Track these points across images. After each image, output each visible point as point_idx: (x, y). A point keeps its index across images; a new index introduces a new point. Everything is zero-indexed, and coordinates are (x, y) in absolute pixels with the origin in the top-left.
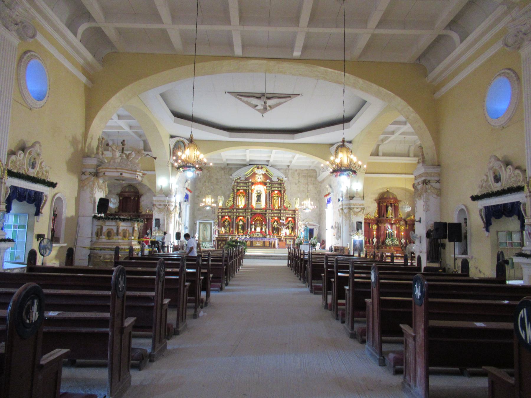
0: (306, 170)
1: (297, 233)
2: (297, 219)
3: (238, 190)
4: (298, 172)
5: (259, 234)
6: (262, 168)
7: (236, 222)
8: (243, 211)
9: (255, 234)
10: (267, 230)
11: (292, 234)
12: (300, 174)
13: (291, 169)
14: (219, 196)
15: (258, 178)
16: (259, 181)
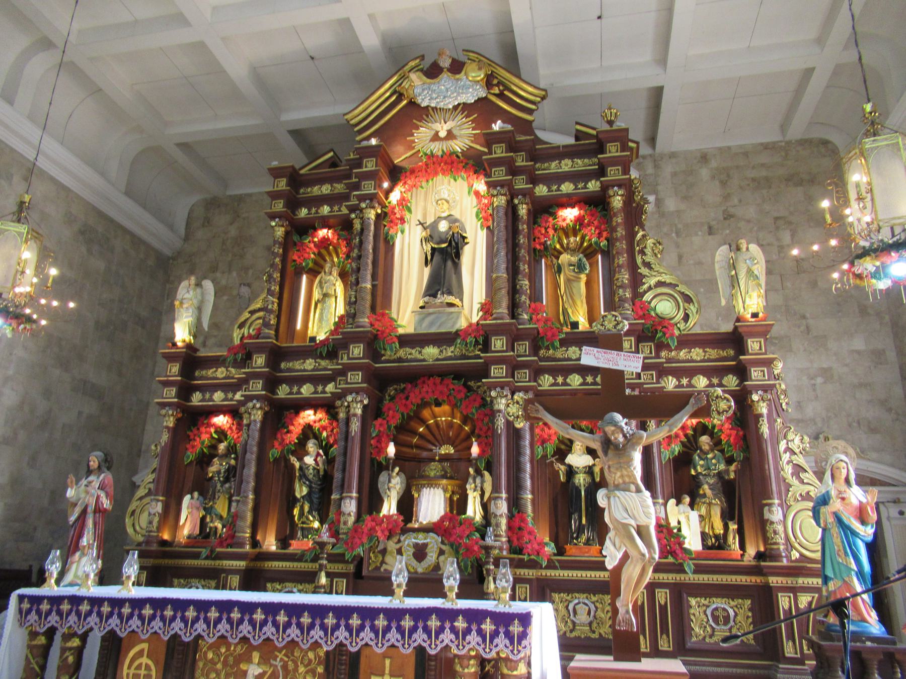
0: (766, 147)
1: (780, 539)
2: (763, 409)
3: (305, 229)
4: (714, 164)
5: (433, 541)
6: (457, 67)
7: (274, 453)
8: (324, 363)
9: (392, 545)
10: (502, 507)
11: (733, 542)
12: (728, 176)
13: (673, 155)
14: (184, 284)
15: (436, 138)
16: (437, 148)
